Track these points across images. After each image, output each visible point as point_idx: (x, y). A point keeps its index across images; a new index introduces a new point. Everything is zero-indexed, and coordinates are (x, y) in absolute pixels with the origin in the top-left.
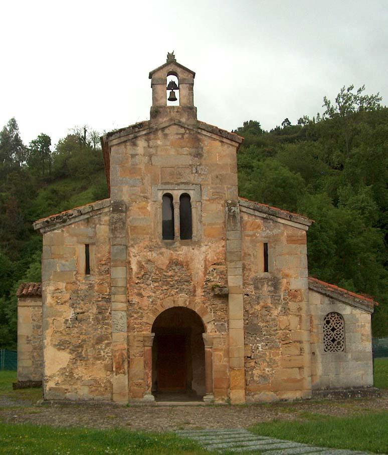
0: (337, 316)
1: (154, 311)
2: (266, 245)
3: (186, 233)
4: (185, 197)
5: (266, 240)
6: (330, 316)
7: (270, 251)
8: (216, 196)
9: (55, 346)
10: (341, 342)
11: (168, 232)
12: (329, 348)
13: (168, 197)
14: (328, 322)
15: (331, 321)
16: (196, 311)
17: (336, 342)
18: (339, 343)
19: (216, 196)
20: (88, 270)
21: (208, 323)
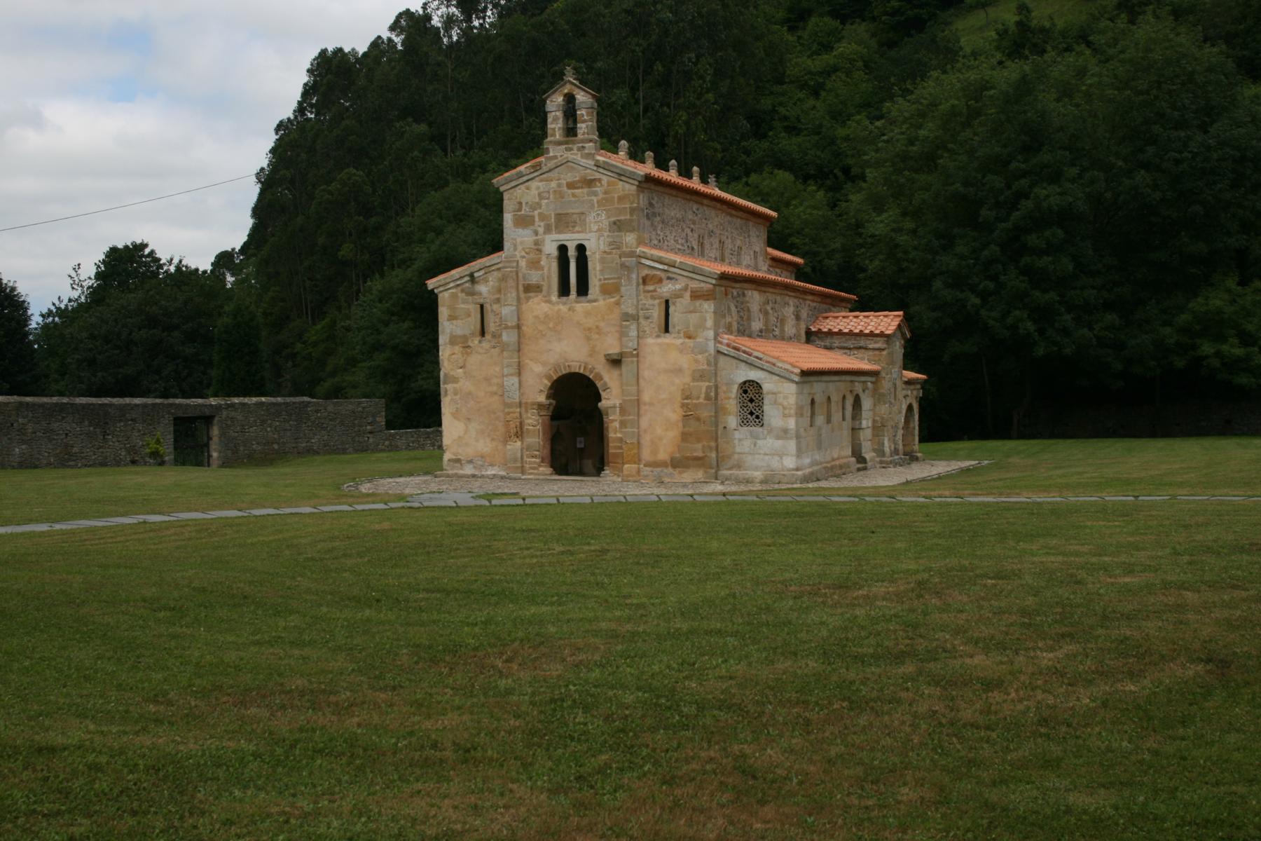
0: (755, 385)
1: (548, 377)
2: (667, 302)
3: (583, 289)
4: (581, 249)
5: (666, 296)
6: (747, 384)
7: (671, 310)
8: (613, 247)
9: (451, 413)
10: (761, 417)
11: (564, 290)
12: (745, 422)
13: (563, 249)
14: (745, 392)
15: (749, 391)
16: (591, 377)
17: (754, 416)
18: (757, 417)
19: (613, 247)
20: (483, 333)
21: (604, 390)
